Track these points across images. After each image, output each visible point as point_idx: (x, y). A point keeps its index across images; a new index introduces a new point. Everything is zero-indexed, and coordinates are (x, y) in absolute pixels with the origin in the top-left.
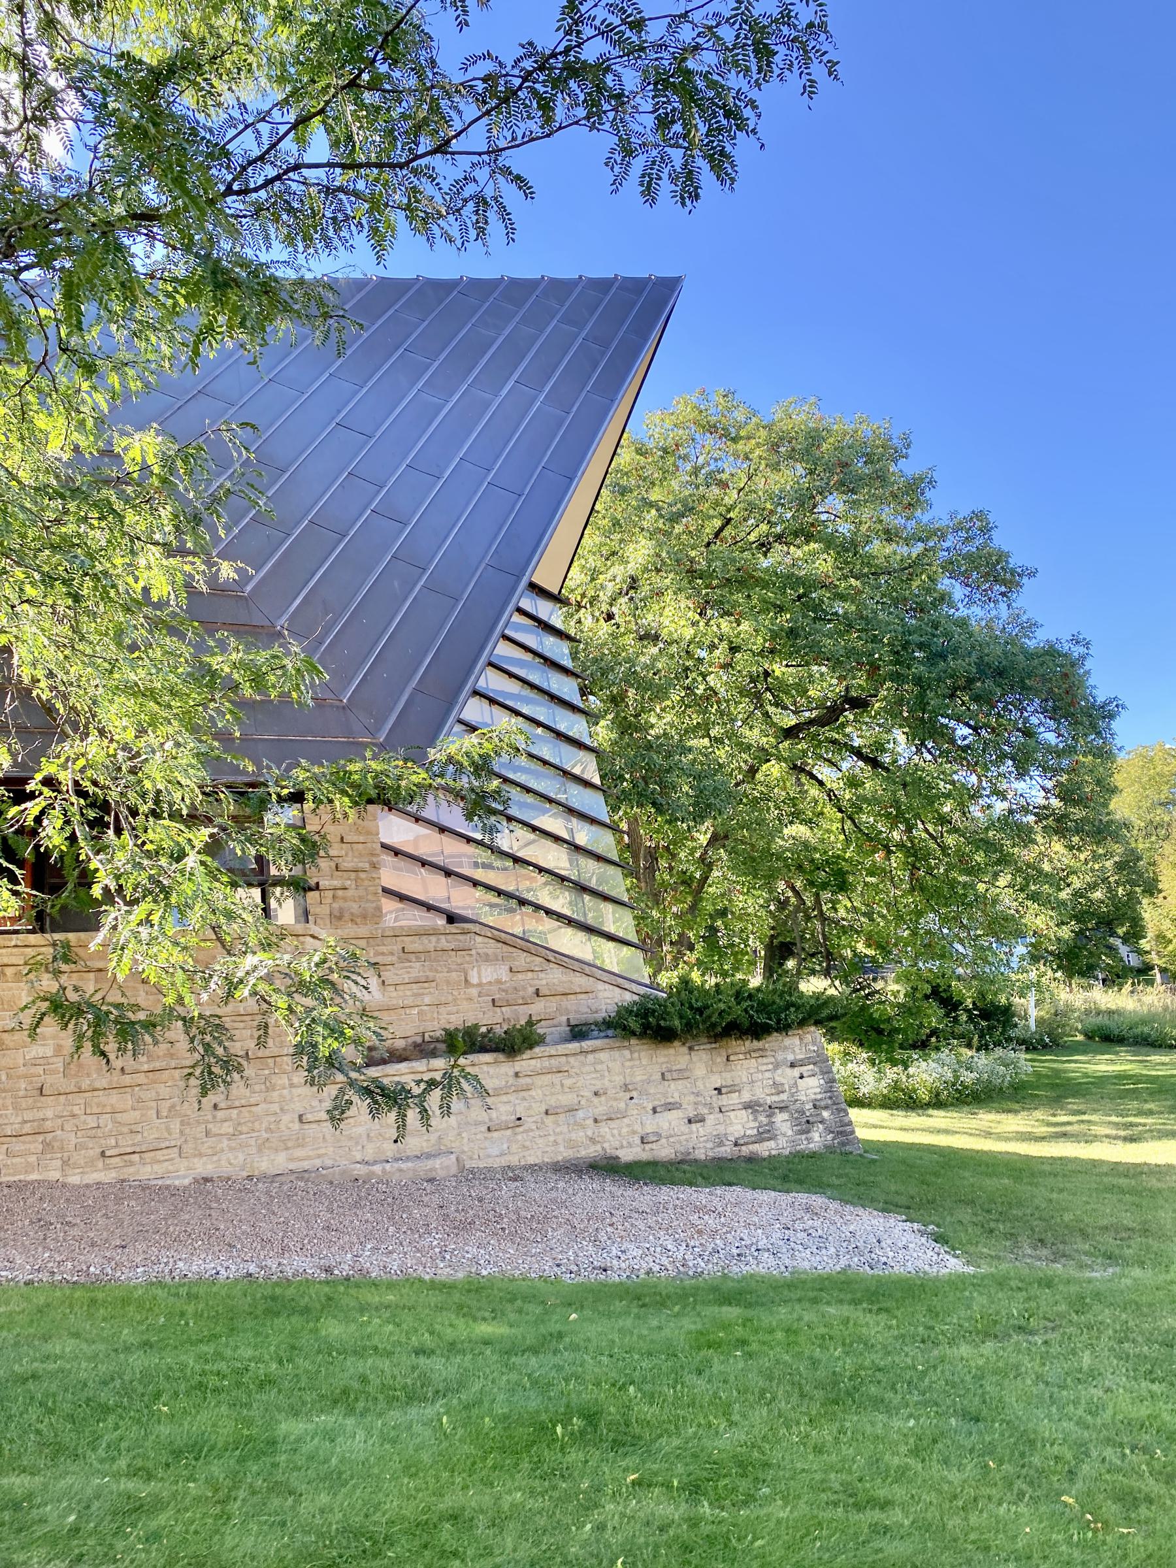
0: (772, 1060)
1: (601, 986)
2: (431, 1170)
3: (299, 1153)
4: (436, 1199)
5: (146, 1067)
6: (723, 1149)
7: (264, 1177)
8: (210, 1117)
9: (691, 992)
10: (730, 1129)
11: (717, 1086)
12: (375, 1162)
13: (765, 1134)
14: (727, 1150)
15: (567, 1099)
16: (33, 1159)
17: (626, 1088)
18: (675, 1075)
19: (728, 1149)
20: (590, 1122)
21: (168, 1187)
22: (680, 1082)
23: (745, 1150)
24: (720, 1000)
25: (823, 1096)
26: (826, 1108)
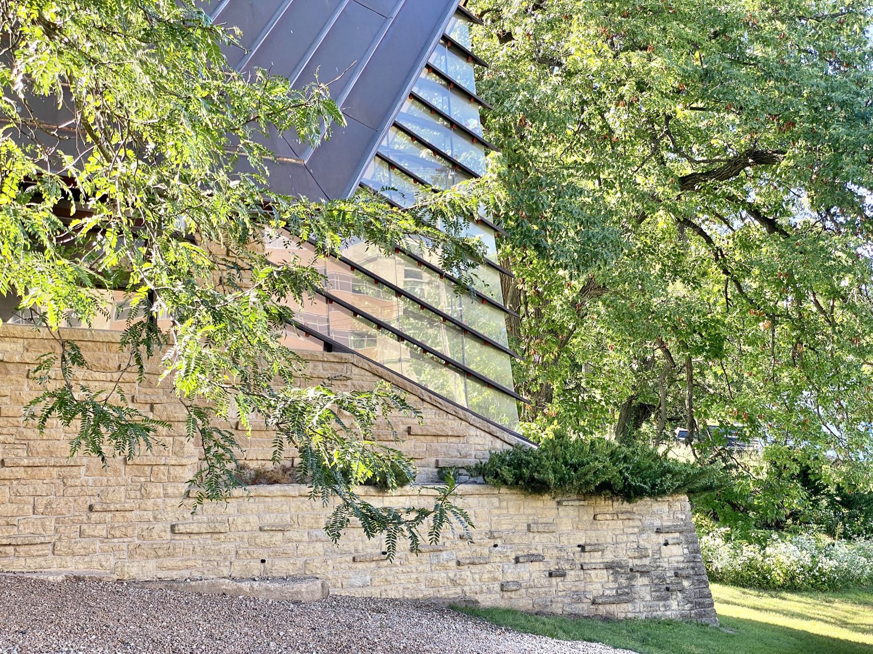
0: (638, 523)
1: (473, 431)
2: (297, 593)
3: (168, 562)
4: (307, 623)
5: (25, 462)
6: (580, 606)
7: (133, 582)
8: (85, 518)
9: (566, 448)
10: (589, 587)
11: (582, 543)
12: (242, 580)
13: (624, 596)
14: (584, 608)
17: (491, 535)
18: (541, 529)
20: (453, 564)
21: (42, 582)
22: (545, 535)
23: (602, 610)
24: (596, 459)
25: (686, 565)
26: (687, 577)
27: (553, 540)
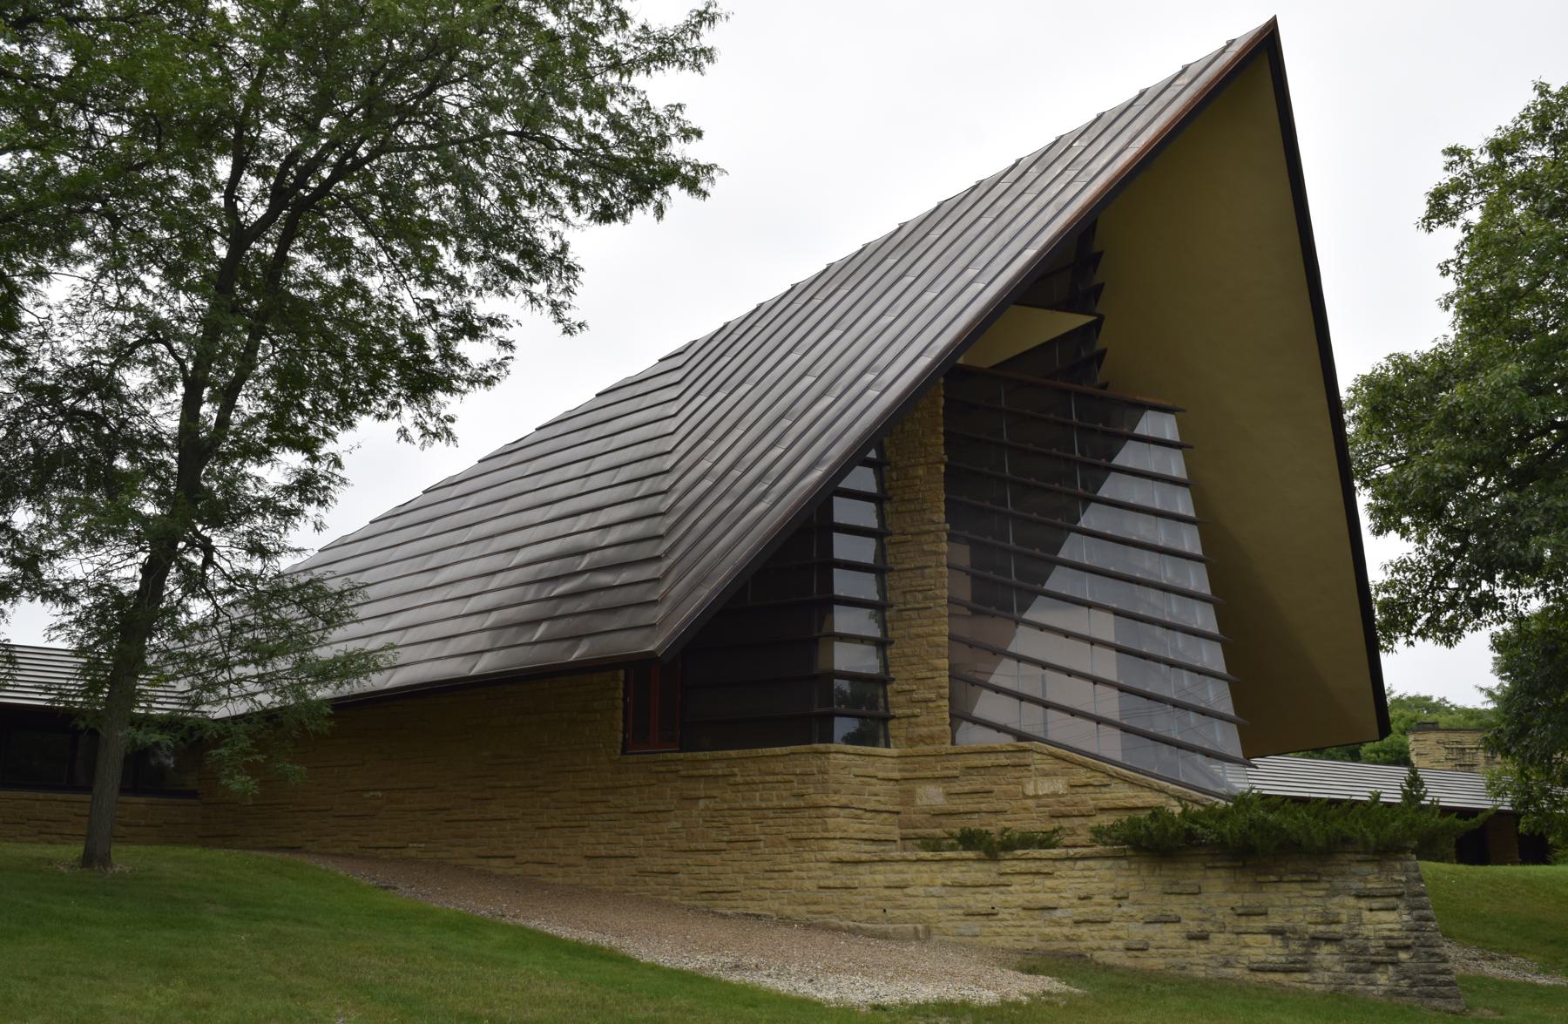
5: (725, 838)
6: (1230, 971)
15: (1046, 898)
16: (666, 888)
19: (1238, 972)
22: (1184, 897)
25: (1405, 934)
26: (1407, 948)
27: (1196, 901)
